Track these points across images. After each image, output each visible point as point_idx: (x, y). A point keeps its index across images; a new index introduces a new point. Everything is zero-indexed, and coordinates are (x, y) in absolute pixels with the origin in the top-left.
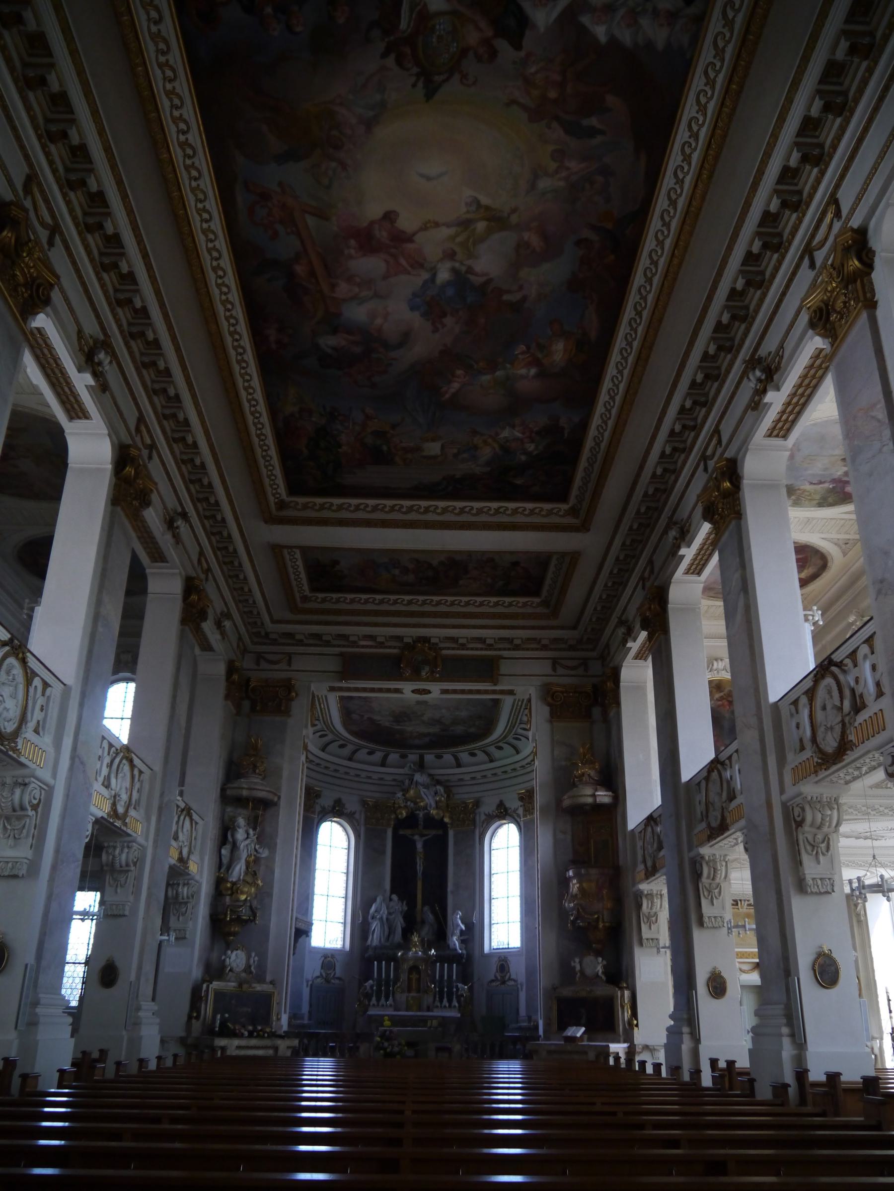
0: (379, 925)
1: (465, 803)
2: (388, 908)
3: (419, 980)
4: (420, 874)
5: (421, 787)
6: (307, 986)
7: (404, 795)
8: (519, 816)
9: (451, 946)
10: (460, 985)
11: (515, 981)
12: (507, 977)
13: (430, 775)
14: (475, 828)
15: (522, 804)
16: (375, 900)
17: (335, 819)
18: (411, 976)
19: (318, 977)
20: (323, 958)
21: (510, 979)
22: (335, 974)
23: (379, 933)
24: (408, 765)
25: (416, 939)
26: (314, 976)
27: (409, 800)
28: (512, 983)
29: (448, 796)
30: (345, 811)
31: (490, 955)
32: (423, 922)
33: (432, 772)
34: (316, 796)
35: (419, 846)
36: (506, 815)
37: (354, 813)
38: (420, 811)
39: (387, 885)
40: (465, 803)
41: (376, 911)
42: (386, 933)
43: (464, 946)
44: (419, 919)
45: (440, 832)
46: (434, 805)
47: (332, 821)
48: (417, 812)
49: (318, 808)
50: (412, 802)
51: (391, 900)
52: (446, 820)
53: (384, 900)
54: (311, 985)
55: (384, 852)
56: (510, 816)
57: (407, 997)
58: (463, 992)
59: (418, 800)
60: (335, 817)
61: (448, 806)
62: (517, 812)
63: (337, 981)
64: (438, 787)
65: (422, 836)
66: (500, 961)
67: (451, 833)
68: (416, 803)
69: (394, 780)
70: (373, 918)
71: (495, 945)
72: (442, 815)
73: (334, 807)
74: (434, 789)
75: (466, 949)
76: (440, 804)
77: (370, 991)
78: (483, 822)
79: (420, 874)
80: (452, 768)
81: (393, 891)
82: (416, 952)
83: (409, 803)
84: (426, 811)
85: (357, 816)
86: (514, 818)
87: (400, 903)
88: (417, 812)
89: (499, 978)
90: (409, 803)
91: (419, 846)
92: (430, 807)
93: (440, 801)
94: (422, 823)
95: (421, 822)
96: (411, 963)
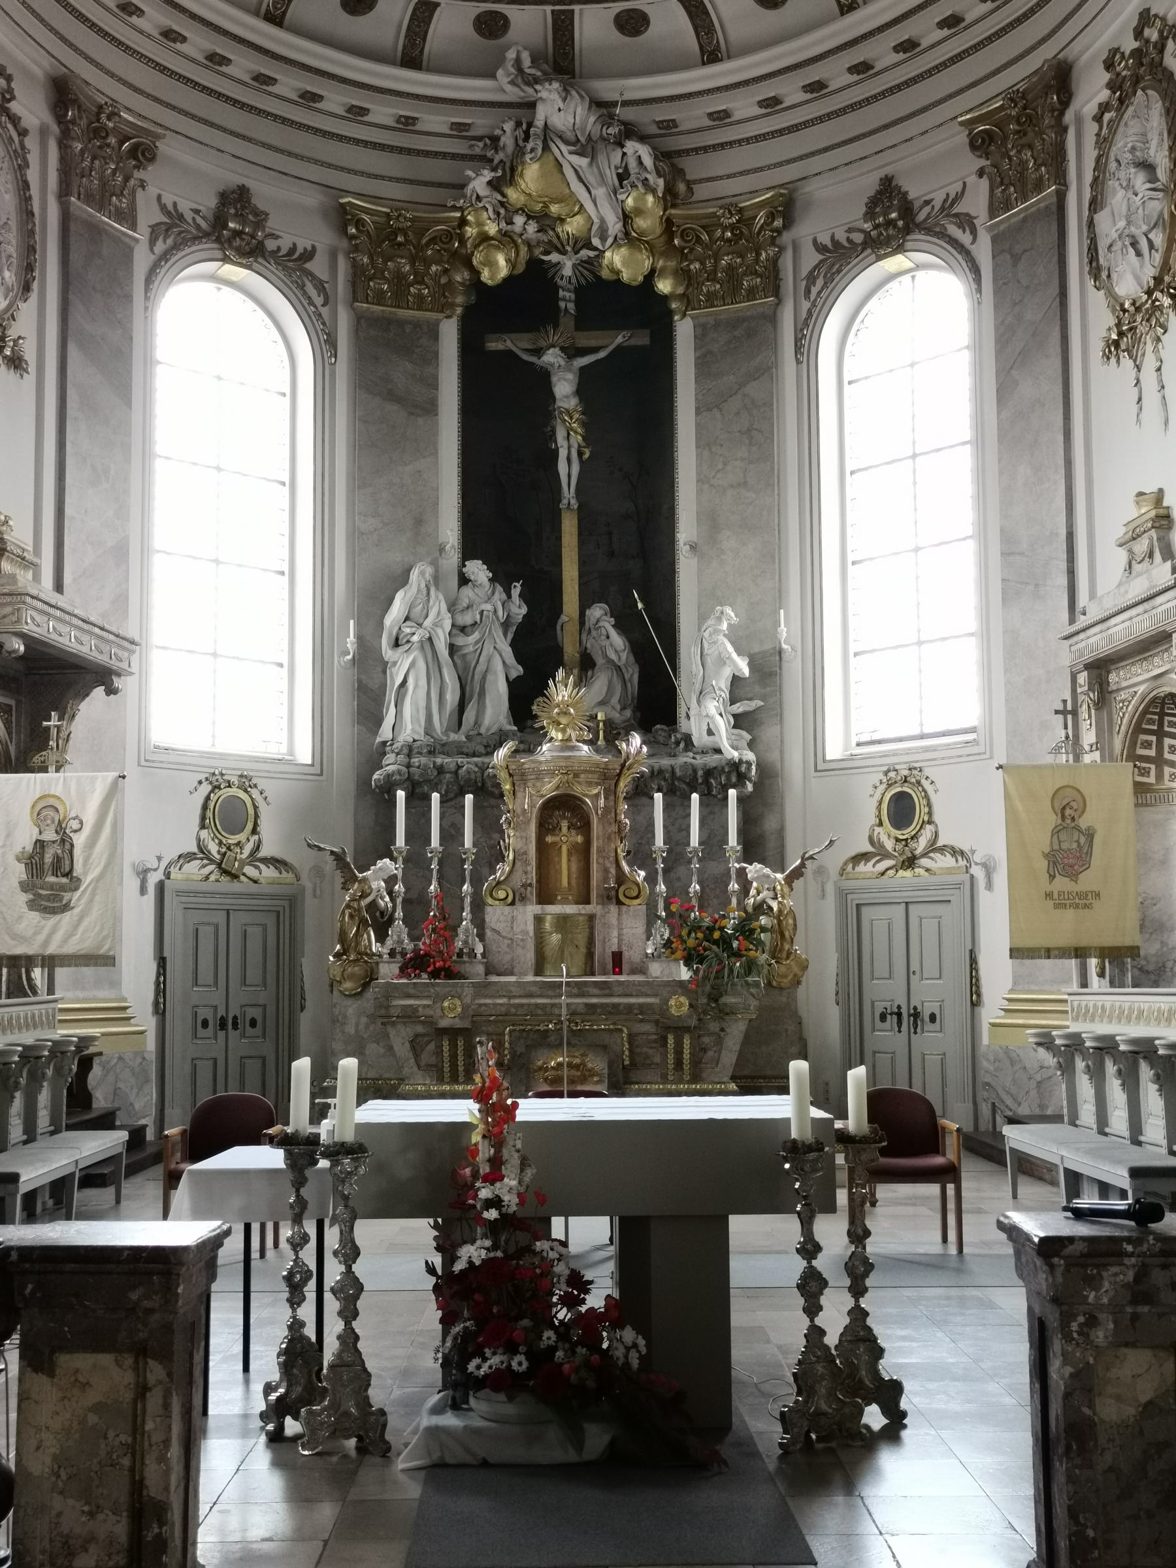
0: (421, 665)
1: (729, 208)
2: (452, 607)
3: (584, 852)
4: (569, 494)
5: (564, 148)
6: (143, 890)
7: (494, 185)
8: (967, 222)
9: (699, 738)
10: (754, 870)
11: (956, 852)
12: (921, 845)
13: (600, 105)
14: (779, 302)
15: (983, 162)
16: (402, 580)
17: (230, 271)
18: (549, 839)
19: (188, 857)
20: (206, 788)
21: (933, 848)
22: (257, 847)
23: (422, 693)
24: (511, 55)
25: (562, 690)
26: (170, 855)
27: (516, 212)
28: (947, 861)
29: (670, 190)
30: (271, 245)
31: (846, 767)
32: (586, 665)
33: (608, 89)
34: (134, 152)
35: (564, 388)
36: (907, 230)
37: (309, 255)
38: (563, 252)
39: (449, 530)
40: (741, 211)
41: (407, 619)
42: (452, 697)
43: (749, 737)
44: (570, 650)
45: (642, 339)
46: (614, 226)
47: (213, 278)
48: (554, 257)
49: (149, 215)
50: (529, 217)
51: (464, 580)
52: (664, 286)
53: (437, 579)
54: (161, 887)
55: (430, 408)
56: (929, 231)
57: (539, 920)
58: (764, 894)
59: (554, 209)
60: (225, 259)
61: (668, 223)
62: (959, 209)
63: (269, 873)
64: (631, 146)
65: (572, 352)
66: (890, 785)
67: (684, 330)
68: (546, 221)
69: (460, 129)
70: (397, 644)
71: (863, 729)
72: (647, 264)
73: (219, 221)
74: (616, 157)
75: (751, 745)
76: (641, 223)
77: (385, 902)
78: (811, 279)
79: (569, 494)
80: (686, 66)
81: (469, 551)
82: (566, 745)
83: (519, 220)
84: (585, 253)
85: (319, 267)
86: (943, 235)
87: (499, 588)
88: (554, 257)
89: (889, 845)
90: (519, 220)
91: (564, 388)
92: (603, 239)
93: (639, 211)
94: (571, 306)
95: (567, 300)
96: (549, 788)
